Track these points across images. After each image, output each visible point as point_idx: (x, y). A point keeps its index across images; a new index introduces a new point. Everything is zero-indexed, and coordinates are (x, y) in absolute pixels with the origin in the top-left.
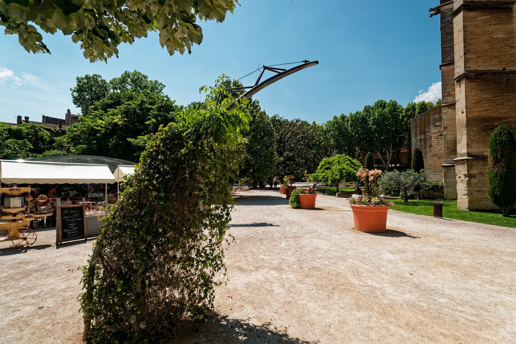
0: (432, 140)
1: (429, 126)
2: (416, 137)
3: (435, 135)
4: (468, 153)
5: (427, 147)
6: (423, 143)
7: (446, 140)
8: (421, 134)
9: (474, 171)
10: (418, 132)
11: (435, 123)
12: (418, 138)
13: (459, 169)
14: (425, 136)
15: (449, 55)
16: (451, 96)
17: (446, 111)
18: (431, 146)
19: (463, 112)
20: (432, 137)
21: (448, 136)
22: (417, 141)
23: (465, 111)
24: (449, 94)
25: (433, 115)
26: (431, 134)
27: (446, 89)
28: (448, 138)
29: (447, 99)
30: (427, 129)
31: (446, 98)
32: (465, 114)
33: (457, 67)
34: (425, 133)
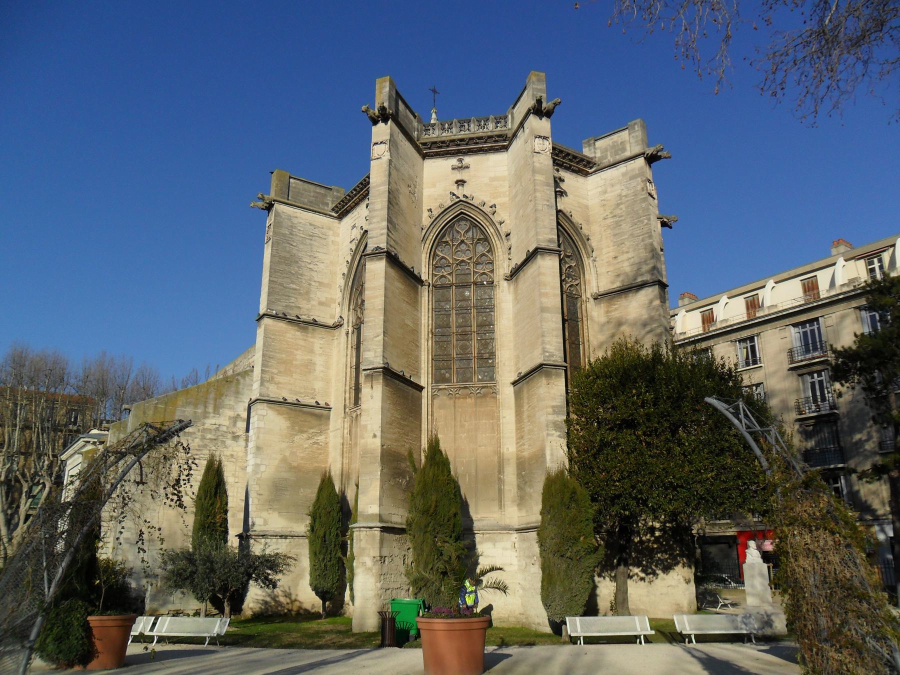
4: (380, 516)
7: (258, 476)
9: (385, 552)
13: (362, 546)
15: (279, 300)
16: (275, 383)
17: (264, 412)
19: (375, 436)
21: (263, 468)
23: (379, 434)
24: (272, 378)
25: (183, 406)
27: (267, 367)
28: (262, 472)
29: (268, 388)
31: (267, 384)
32: (378, 441)
33: (369, 350)
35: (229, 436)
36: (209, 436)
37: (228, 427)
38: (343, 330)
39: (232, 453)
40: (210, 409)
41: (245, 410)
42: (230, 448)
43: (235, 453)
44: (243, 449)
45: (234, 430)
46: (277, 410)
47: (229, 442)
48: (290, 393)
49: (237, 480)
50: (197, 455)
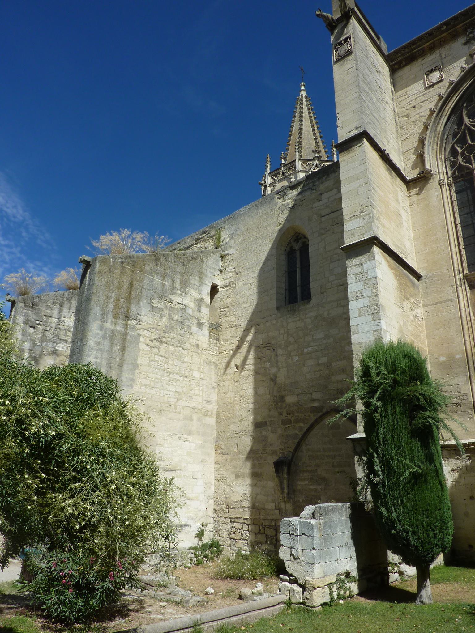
0: (142, 346)
1: (138, 303)
2: (103, 319)
3: (147, 333)
5: (126, 368)
6: (117, 348)
8: (116, 316)
10: (111, 307)
11: (151, 298)
12: (108, 325)
14: (126, 326)
18: (136, 366)
20: (142, 339)
22: (104, 337)
25: (151, 274)
26: (139, 327)
30: (133, 309)
34: (127, 318)
35: (195, 322)
36: (176, 317)
37: (193, 311)
38: (433, 184)
39: (198, 342)
40: (177, 285)
41: (208, 294)
42: (196, 337)
43: (199, 343)
44: (207, 340)
45: (200, 314)
46: (388, 262)
47: (194, 329)
48: (393, 244)
49: (202, 377)
50: (164, 337)
